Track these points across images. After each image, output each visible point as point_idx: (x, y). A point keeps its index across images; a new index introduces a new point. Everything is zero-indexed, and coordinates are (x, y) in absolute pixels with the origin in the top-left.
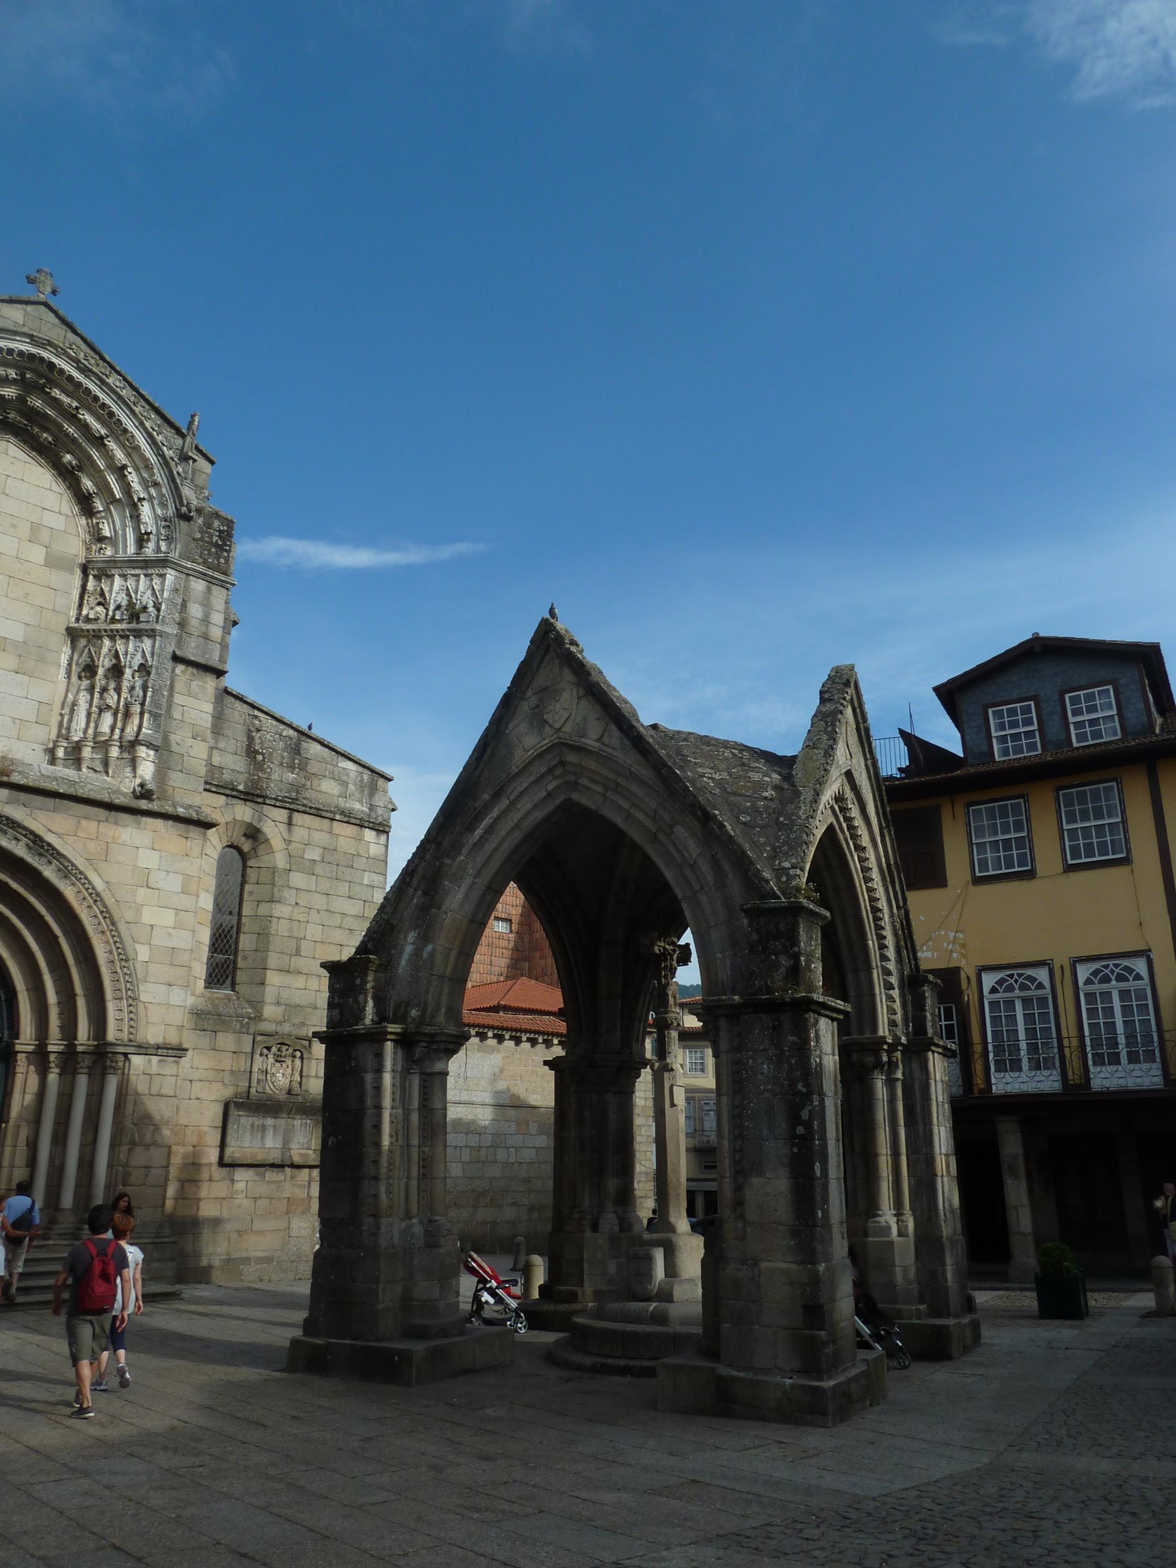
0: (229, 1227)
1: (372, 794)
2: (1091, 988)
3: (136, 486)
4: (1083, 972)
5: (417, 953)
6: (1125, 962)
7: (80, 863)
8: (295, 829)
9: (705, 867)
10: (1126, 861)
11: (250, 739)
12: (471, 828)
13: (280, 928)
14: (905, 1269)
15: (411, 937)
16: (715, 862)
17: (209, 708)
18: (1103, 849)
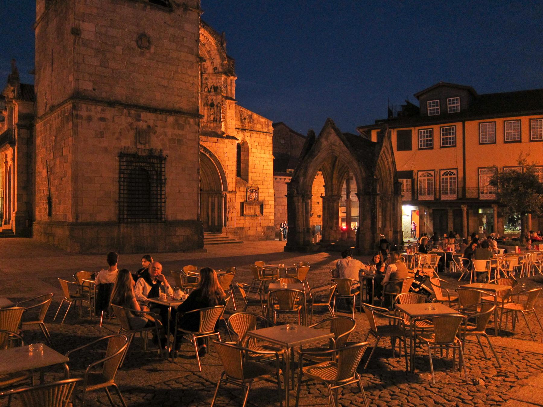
0: (246, 229)
1: (268, 127)
2: (443, 177)
3: (212, 55)
4: (442, 172)
5: (303, 181)
6: (452, 171)
7: (214, 153)
8: (252, 138)
9: (358, 170)
10: (455, 146)
11: (241, 116)
12: (313, 158)
13: (251, 163)
14: (391, 236)
15: (302, 178)
16: (360, 169)
17: (234, 112)
18: (450, 143)
